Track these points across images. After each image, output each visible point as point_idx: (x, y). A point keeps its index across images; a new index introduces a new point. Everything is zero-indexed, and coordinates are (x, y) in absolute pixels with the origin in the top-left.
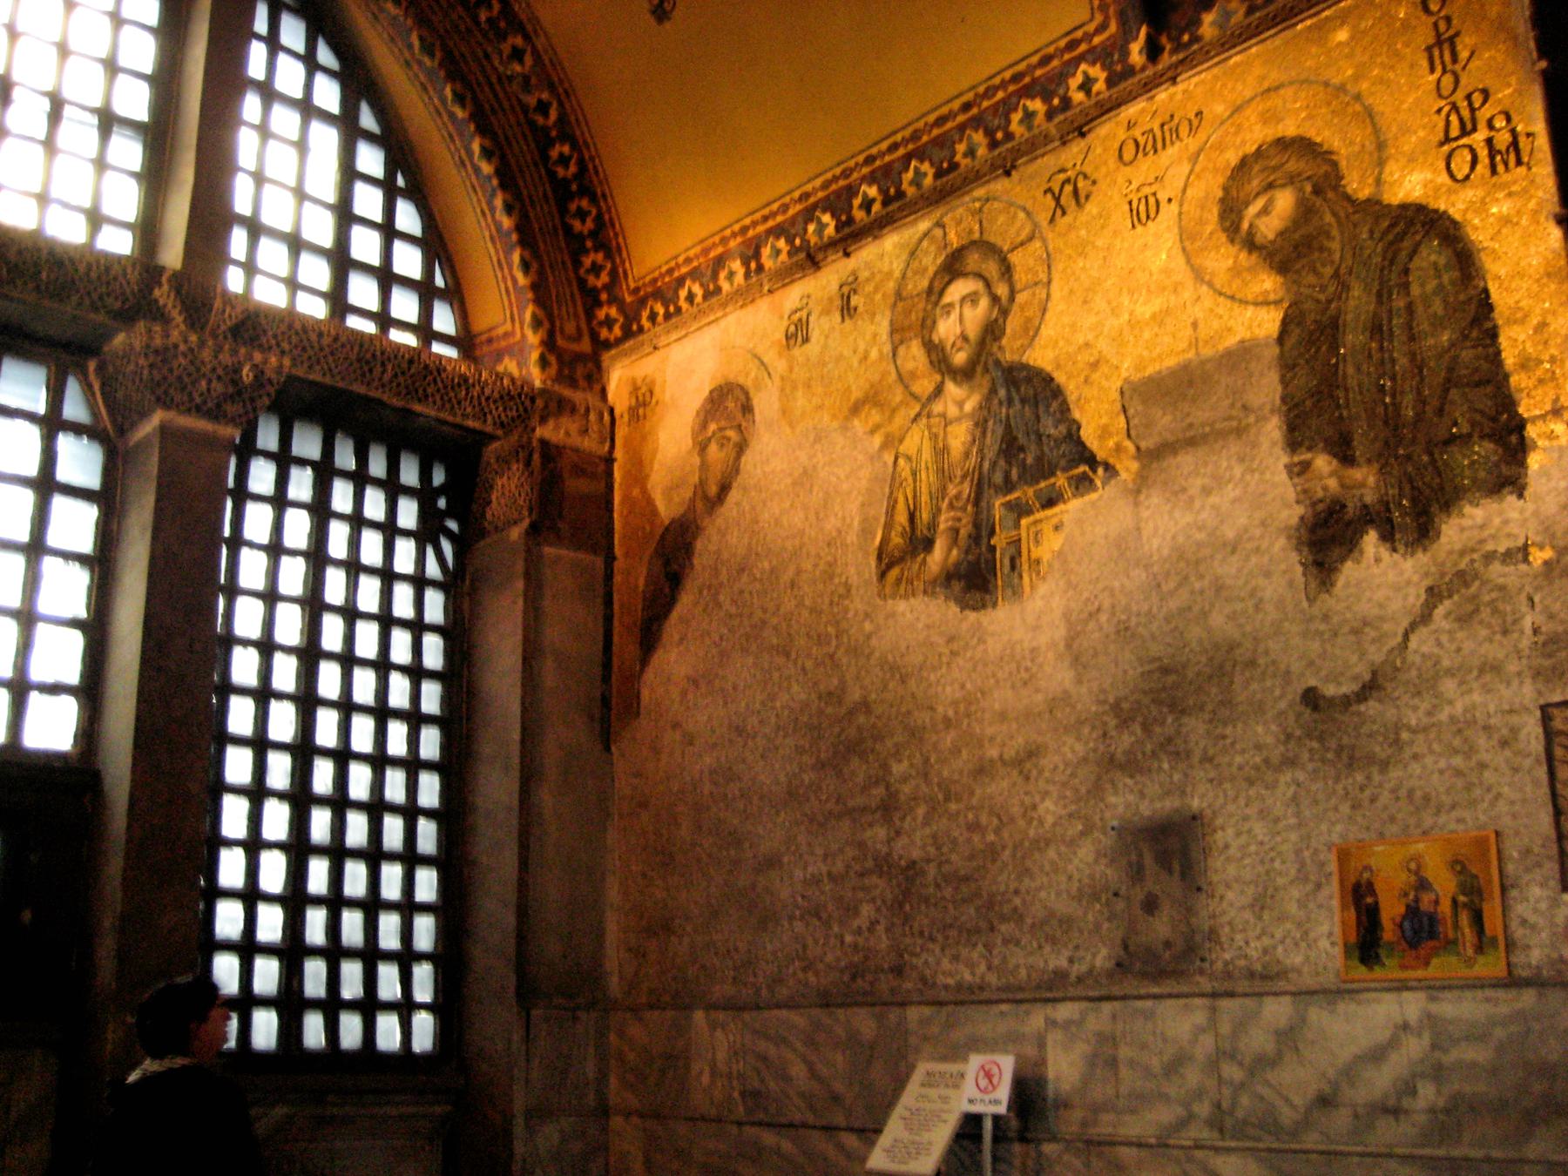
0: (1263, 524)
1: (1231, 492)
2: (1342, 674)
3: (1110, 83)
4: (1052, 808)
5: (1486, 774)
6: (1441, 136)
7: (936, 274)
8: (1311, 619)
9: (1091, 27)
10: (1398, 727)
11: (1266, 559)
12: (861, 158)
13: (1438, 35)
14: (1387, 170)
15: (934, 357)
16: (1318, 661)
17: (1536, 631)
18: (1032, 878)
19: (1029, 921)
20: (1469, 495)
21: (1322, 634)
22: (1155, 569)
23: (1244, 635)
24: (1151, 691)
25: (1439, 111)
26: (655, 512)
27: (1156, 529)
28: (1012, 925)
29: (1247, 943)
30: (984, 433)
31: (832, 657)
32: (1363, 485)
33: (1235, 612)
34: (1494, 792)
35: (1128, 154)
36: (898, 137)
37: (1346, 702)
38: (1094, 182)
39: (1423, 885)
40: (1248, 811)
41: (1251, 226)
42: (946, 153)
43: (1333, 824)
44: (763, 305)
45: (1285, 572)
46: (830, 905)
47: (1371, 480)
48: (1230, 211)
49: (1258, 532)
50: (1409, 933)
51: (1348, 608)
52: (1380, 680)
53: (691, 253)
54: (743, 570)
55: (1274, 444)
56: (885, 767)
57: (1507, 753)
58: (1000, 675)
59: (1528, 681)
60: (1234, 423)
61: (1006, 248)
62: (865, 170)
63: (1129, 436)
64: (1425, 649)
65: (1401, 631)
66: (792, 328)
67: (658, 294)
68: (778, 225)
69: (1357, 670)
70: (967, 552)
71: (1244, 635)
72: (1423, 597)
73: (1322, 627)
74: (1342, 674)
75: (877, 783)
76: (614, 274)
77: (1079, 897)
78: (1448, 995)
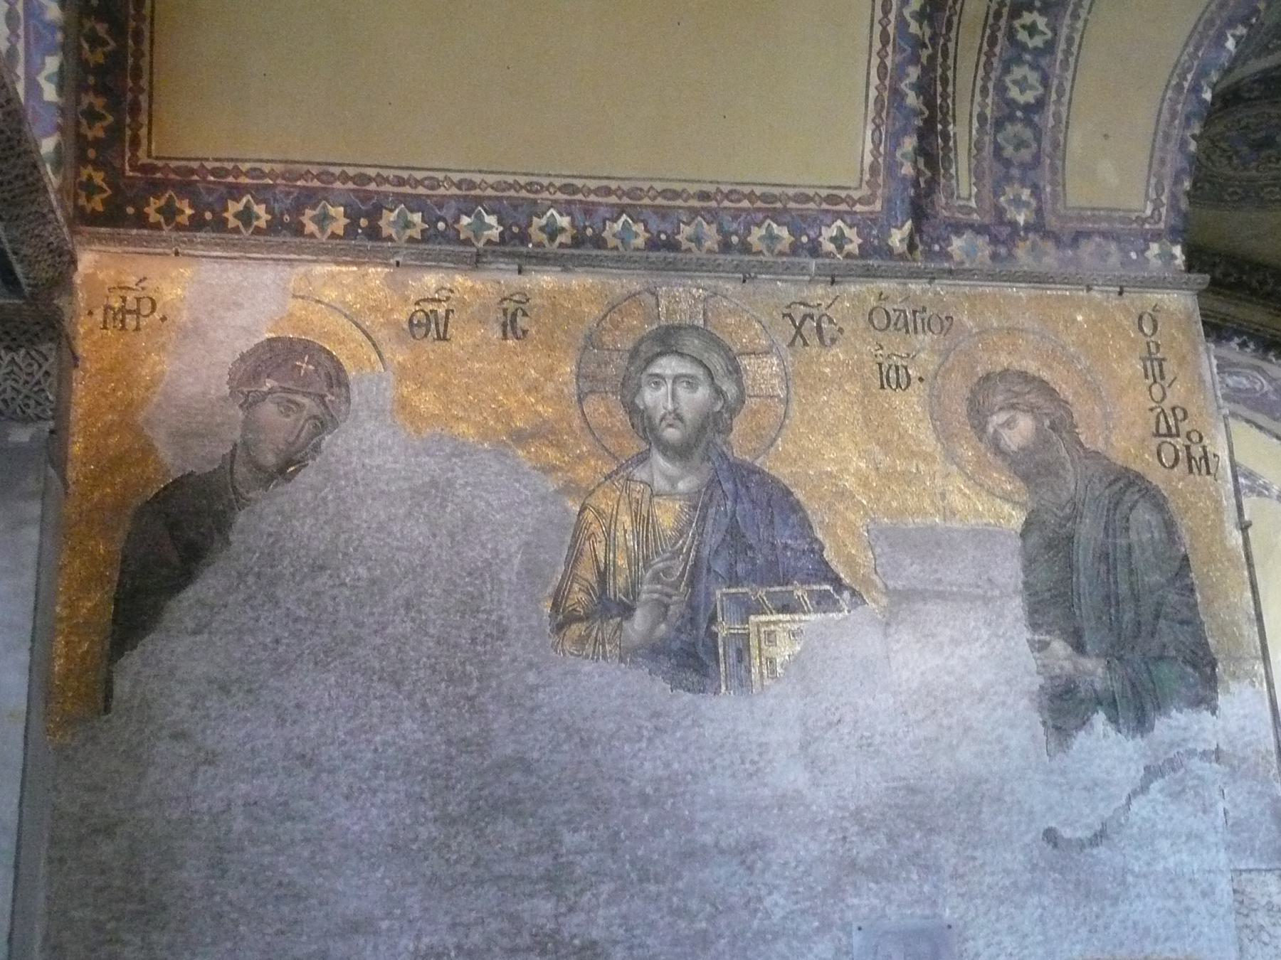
0: (1008, 682)
3: (865, 252)
4: (782, 901)
5: (1191, 916)
6: (1154, 430)
7: (641, 341)
8: (1052, 771)
9: (856, 195)
10: (1125, 871)
11: (1011, 713)
12: (558, 182)
13: (1149, 351)
15: (637, 421)
17: (1225, 812)
20: (1175, 702)
21: (1060, 786)
22: (903, 698)
24: (897, 806)
25: (1151, 410)
26: (148, 450)
30: (703, 518)
31: (470, 699)
32: (1092, 673)
33: (982, 752)
35: (879, 320)
36: (613, 185)
37: (1081, 845)
40: (998, 926)
41: (996, 431)
42: (667, 227)
44: (376, 274)
45: (1029, 728)
47: (1100, 671)
48: (978, 414)
52: (1109, 831)
53: (266, 168)
54: (322, 568)
55: (1017, 620)
57: (1207, 902)
58: (718, 761)
60: (980, 591)
61: (736, 348)
62: (560, 196)
64: (1144, 813)
66: (420, 314)
67: (186, 188)
68: (419, 196)
69: (1089, 821)
70: (679, 630)
73: (1061, 780)
75: (540, 850)
76: (115, 132)
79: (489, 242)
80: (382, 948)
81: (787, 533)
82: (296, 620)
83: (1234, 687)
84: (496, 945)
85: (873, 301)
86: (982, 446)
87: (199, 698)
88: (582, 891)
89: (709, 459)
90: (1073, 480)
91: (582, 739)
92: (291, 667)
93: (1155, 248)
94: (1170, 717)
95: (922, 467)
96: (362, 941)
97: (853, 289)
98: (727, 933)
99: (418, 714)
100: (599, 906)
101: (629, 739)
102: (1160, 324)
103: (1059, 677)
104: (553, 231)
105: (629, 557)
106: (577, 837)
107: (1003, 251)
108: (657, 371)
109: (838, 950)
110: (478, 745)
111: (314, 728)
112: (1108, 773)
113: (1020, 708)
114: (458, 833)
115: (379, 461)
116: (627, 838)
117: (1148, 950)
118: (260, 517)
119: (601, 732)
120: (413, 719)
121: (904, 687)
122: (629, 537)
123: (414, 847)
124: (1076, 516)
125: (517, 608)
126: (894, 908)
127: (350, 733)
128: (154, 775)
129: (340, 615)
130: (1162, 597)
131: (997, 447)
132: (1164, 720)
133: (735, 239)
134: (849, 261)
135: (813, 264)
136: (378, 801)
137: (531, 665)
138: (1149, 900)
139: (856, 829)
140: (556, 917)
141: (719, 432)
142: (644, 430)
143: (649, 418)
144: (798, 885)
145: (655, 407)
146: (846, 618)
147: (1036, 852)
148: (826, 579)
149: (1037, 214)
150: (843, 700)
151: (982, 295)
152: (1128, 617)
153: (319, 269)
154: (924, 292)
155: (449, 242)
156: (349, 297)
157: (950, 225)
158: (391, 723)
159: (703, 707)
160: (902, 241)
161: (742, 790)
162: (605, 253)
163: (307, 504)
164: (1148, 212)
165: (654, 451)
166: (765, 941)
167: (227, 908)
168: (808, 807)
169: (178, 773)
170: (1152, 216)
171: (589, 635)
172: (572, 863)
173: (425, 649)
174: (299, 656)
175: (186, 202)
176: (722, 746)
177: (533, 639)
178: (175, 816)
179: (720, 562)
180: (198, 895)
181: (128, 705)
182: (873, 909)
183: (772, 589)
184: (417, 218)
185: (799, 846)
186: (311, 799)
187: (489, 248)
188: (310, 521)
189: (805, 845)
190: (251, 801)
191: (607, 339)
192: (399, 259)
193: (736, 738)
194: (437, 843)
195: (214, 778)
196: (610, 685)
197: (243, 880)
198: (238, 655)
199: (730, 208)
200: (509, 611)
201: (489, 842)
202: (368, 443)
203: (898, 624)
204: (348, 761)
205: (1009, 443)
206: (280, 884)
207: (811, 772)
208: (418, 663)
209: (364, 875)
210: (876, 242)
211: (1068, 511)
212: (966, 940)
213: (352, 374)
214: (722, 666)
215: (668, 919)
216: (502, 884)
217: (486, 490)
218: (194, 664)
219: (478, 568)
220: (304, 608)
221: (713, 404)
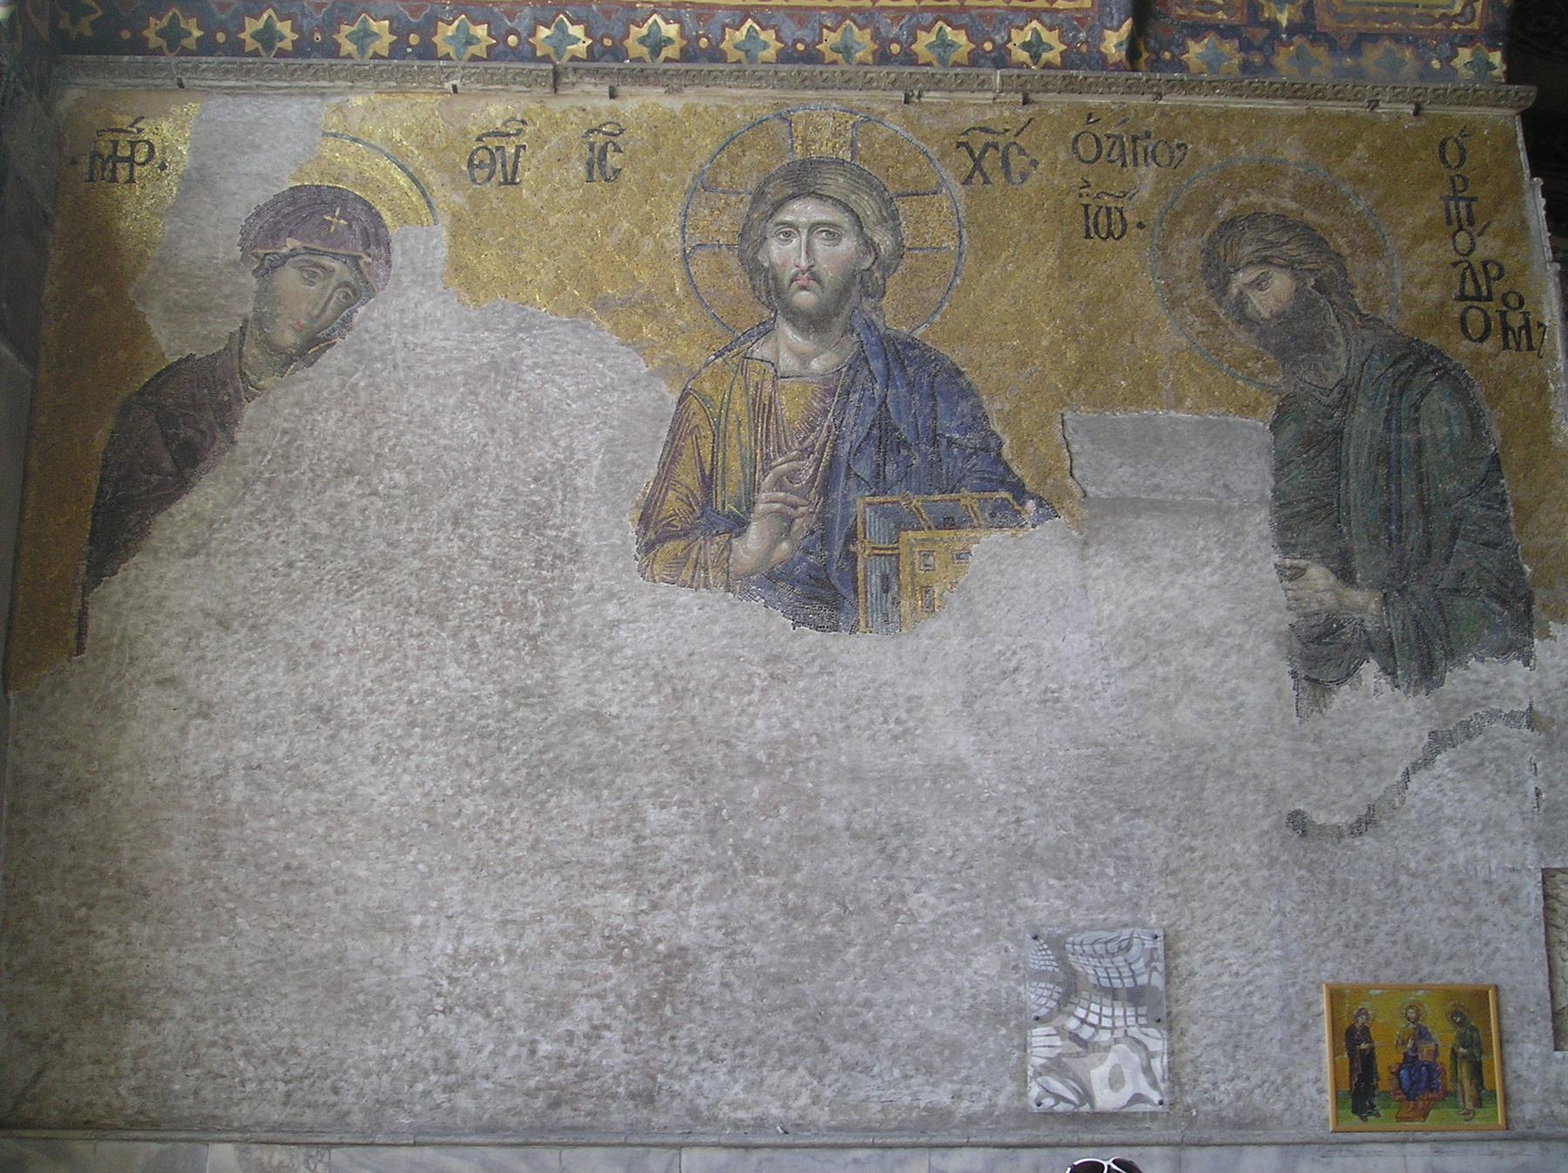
0: (1246, 620)
2: (1334, 803)
3: (1068, 61)
4: (932, 901)
5: (1485, 928)
6: (1456, 291)
7: (767, 182)
8: (1303, 737)
11: (1249, 662)
15: (760, 282)
17: (1538, 794)
18: (896, 987)
19: (888, 1042)
21: (1314, 755)
23: (1219, 737)
24: (1090, 779)
25: (1455, 264)
26: (136, 330)
27: (1108, 597)
28: (860, 1045)
29: (1215, 1084)
31: (532, 638)
33: (1208, 711)
34: (1492, 947)
35: (1087, 149)
38: (1035, 163)
39: (1422, 1034)
40: (1221, 937)
41: (1241, 293)
43: (1323, 961)
45: (1273, 680)
46: (510, 997)
48: (1216, 271)
50: (1406, 1083)
54: (350, 473)
55: (1263, 538)
56: (634, 812)
57: (1507, 910)
58: (853, 719)
59: (1532, 843)
61: (891, 192)
64: (1425, 792)
65: (1401, 769)
66: (483, 155)
69: (1351, 801)
72: (1427, 739)
74: (1334, 803)
75: (616, 830)
77: (974, 1014)
78: (1452, 1147)
79: (574, 58)
80: (413, 948)
81: (954, 424)
82: (315, 538)
83: (1555, 628)
84: (557, 948)
85: (1079, 126)
87: (193, 635)
88: (670, 883)
89: (853, 331)
91: (674, 690)
92: (306, 598)
93: (1465, 54)
94: (1467, 668)
95: (1139, 341)
96: (388, 940)
98: (860, 940)
99: (466, 657)
100: (690, 903)
101: (736, 690)
104: (656, 44)
105: (743, 457)
106: (664, 815)
107: (1257, 59)
108: (788, 218)
109: (1005, 965)
110: (541, 696)
111: (334, 673)
112: (1379, 739)
113: (1263, 653)
114: (512, 807)
115: (425, 338)
116: (731, 817)
117: (1425, 970)
118: (275, 410)
119: (701, 682)
120: (459, 664)
121: (1106, 626)
122: (744, 432)
123: (456, 824)
125: (595, 522)
126: (1082, 911)
127: (379, 679)
128: (136, 729)
129: (370, 532)
132: (1458, 671)
133: (895, 48)
134: (1045, 72)
135: (997, 76)
136: (411, 764)
137: (611, 595)
138: (1429, 907)
139: (1035, 809)
140: (635, 915)
141: (868, 295)
142: (768, 293)
143: (775, 278)
144: (955, 881)
145: (784, 265)
146: (1031, 534)
147: (1276, 844)
148: (1002, 483)
149: (1305, 12)
150: (1022, 641)
151: (1227, 115)
153: (358, 101)
155: (522, 59)
156: (398, 136)
157: (1184, 26)
158: (429, 666)
159: (834, 650)
160: (1120, 44)
161: (884, 758)
162: (720, 66)
163: (333, 393)
164: (1458, 9)
165: (780, 319)
166: (910, 953)
167: (223, 895)
168: (970, 780)
169: (164, 728)
170: (1461, 14)
171: (687, 557)
172: (656, 847)
173: (476, 575)
174: (317, 583)
175: (193, 21)
176: (858, 701)
177: (613, 562)
178: (161, 781)
179: (862, 463)
180: (188, 878)
181: (104, 644)
182: (1054, 912)
183: (932, 498)
184: (481, 31)
185: (957, 830)
186: (327, 762)
187: (571, 64)
188: (335, 414)
189: (967, 828)
190: (255, 764)
191: (724, 179)
192: (455, 82)
193: (877, 690)
194: (484, 821)
195: (210, 732)
196: (714, 621)
197: (242, 861)
198: (241, 581)
199: (889, 8)
200: (586, 526)
201: (551, 819)
202: (412, 316)
203: (1100, 544)
204: (375, 716)
205: (1258, 307)
206: (288, 867)
207: (977, 735)
208: (466, 592)
209: (392, 857)
210: (1084, 49)
212: (1176, 955)
213: (393, 232)
214: (861, 596)
215: (781, 920)
216: (567, 872)
217: (564, 375)
218: (188, 593)
219: (546, 471)
220: (325, 524)
221: (864, 259)
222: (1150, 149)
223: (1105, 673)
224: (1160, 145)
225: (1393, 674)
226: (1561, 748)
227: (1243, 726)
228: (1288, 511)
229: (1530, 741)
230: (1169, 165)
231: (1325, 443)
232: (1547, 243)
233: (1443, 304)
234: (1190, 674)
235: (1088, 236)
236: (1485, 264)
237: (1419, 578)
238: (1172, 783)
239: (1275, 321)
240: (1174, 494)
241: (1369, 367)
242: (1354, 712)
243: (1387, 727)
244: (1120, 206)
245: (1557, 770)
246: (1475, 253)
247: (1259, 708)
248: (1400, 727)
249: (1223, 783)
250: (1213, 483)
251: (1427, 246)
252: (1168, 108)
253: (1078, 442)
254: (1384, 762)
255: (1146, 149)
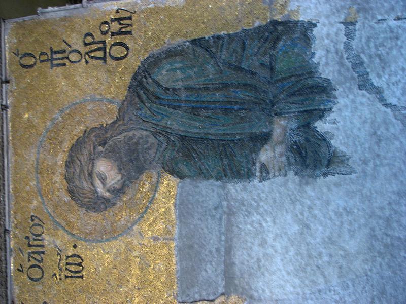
0: (293, 202)
1: (268, 224)
8: (364, 172)
11: (318, 202)
13: (47, 60)
14: (109, 96)
16: (394, 171)
17: (398, 19)
21: (375, 165)
23: (366, 225)
25: (87, 62)
27: (281, 287)
32: (284, 129)
33: (349, 231)
41: (108, 191)
45: (329, 189)
47: (282, 122)
48: (98, 204)
49: (299, 207)
51: (362, 145)
55: (245, 189)
63: (213, 301)
64: (399, 93)
65: (383, 109)
71: (366, 225)
72: (364, 92)
73: (371, 164)
83: (293, 6)
86: (119, 204)
90: (141, 132)
94: (319, 63)
95: (136, 253)
97: (17, 291)
102: (27, 52)
103: (288, 158)
112: (365, 122)
113: (313, 194)
121: (299, 290)
124: (164, 132)
130: (225, 63)
131: (119, 191)
152: (241, 95)
154: (15, 236)
203: (251, 289)
205: (115, 181)
211: (162, 139)
222: (35, 237)
223: (328, 292)
224: (32, 231)
225: (324, 111)
226: (368, 3)
227: (358, 210)
228: (229, 171)
229: (363, 23)
230: (42, 227)
231: (189, 147)
232: (72, 6)
233: (109, 71)
234: (327, 239)
235: (82, 277)
236: (86, 44)
237: (265, 92)
238: (396, 258)
239: (123, 171)
240: (221, 240)
241: (145, 117)
242: (348, 138)
243: (356, 116)
244: (65, 258)
245: (383, 6)
246: (80, 50)
247: (346, 198)
248: (356, 108)
249: (395, 225)
250: (214, 216)
251: (78, 78)
252: (13, 225)
253: (194, 295)
254: (378, 120)
255: (35, 240)
